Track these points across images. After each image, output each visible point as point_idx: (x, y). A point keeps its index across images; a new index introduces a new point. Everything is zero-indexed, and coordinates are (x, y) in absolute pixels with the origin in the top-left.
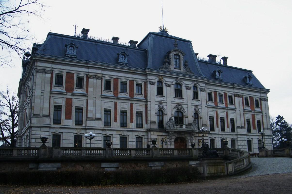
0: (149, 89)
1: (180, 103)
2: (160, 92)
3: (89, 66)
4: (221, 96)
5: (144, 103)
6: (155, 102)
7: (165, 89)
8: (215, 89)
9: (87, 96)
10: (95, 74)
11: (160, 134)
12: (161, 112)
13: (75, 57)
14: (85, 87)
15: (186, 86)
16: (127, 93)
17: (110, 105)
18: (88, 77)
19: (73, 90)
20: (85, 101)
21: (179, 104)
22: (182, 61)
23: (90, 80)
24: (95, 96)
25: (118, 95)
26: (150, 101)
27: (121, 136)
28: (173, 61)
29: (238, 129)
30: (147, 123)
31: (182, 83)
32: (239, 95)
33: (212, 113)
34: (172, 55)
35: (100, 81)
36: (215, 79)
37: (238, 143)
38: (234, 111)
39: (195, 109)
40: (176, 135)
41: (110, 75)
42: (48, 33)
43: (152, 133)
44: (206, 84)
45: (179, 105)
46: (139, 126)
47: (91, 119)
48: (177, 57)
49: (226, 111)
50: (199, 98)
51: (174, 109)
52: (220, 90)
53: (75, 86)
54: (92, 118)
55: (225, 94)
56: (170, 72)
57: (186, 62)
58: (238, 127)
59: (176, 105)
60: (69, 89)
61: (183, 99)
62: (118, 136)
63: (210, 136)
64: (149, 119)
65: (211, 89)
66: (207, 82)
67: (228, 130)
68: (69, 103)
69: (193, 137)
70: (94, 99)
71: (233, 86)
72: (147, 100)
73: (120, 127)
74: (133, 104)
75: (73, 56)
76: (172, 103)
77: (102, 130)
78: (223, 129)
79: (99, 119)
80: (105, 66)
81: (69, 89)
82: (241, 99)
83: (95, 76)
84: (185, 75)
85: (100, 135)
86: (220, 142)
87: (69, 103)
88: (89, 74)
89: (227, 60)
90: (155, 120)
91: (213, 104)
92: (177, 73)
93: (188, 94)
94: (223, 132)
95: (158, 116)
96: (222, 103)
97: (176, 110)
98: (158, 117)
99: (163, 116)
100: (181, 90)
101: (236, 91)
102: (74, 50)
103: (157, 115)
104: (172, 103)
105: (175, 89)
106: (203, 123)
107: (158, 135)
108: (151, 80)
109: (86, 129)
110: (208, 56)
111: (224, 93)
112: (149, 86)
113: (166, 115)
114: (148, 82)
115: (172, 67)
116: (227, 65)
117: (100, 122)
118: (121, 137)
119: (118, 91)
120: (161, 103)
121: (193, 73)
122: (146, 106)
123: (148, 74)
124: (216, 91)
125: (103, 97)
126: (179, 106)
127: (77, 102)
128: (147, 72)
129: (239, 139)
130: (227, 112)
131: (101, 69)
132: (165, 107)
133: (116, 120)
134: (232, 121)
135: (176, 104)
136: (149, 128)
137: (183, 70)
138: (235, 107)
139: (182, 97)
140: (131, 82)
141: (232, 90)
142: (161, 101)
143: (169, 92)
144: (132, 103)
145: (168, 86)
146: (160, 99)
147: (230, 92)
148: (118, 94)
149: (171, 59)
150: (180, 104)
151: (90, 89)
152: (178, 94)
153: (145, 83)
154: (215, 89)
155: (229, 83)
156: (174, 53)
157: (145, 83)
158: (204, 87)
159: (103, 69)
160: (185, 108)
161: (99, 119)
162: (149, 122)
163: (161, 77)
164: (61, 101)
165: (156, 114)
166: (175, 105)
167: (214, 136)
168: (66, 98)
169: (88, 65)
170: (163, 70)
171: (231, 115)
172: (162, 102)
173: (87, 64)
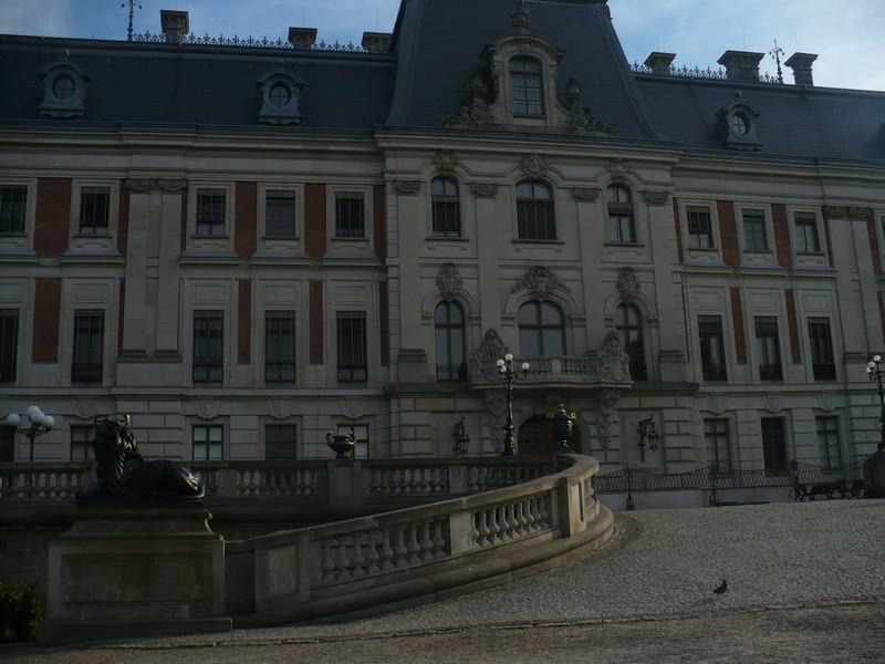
0: (391, 212)
1: (541, 264)
2: (447, 219)
3: (129, 146)
4: (754, 218)
5: (375, 276)
6: (423, 265)
8: (725, 192)
9: (123, 266)
10: (156, 175)
11: (446, 404)
12: (452, 310)
13: (72, 118)
14: (113, 231)
15: (573, 189)
16: (297, 240)
17: (219, 293)
18: (126, 190)
20: (114, 286)
21: (538, 271)
22: (552, 83)
23: (135, 199)
24: (153, 262)
25: (254, 250)
26: (398, 266)
27: (270, 422)
28: (506, 86)
29: (848, 366)
30: (385, 361)
31: (551, 174)
32: (848, 208)
33: (712, 300)
34: (502, 59)
35: (178, 198)
36: (725, 146)
37: (853, 431)
38: (829, 285)
39: (619, 286)
40: (527, 409)
41: (219, 168)
43: (407, 403)
44: (675, 170)
45: (539, 272)
48: (529, 67)
49: (783, 285)
50: (642, 236)
51: (513, 292)
52: (750, 194)
53: (74, 229)
54: (143, 352)
55: (779, 210)
56: (496, 131)
57: (572, 82)
58: (847, 357)
59: (527, 276)
60: (51, 243)
61: (558, 247)
62: (254, 422)
63: (703, 404)
64: (393, 342)
65: (704, 190)
66: (676, 160)
67: (799, 373)
68: (48, 294)
69: (606, 411)
70: (152, 272)
71: (817, 170)
72: (384, 262)
73: (263, 384)
74: (321, 281)
75: (69, 115)
76: (501, 267)
77: (183, 398)
78: (772, 373)
79: (172, 356)
80: (196, 139)
82: (861, 226)
83: (157, 180)
84: (567, 135)
85: (171, 421)
86: (758, 428)
87: (48, 294)
88: (133, 175)
89: (816, 67)
90: (421, 348)
91: (713, 258)
92: (526, 134)
93: (581, 223)
94: (769, 382)
95: (438, 326)
96: (766, 250)
97: (528, 298)
98: (445, 331)
99: (462, 326)
100: (549, 205)
101: (831, 190)
102: (73, 90)
103: (432, 322)
104: (501, 267)
105: (520, 203)
106: (663, 349)
107: (433, 412)
108: (399, 177)
109: (114, 398)
110: (721, 61)
111: (772, 204)
112: (391, 199)
113: (475, 322)
114: (389, 186)
115: (499, 113)
116: (815, 84)
117: (173, 367)
118: (267, 426)
119: (255, 236)
120: (448, 267)
121: (608, 131)
122: (383, 287)
123: (386, 153)
124: (731, 197)
125: (186, 263)
126: (541, 276)
127: (79, 291)
128: (381, 145)
129: (856, 412)
130: (789, 294)
131: (182, 151)
132: (469, 286)
133: (244, 357)
134: (820, 330)
135: (525, 267)
136: (392, 381)
137: (557, 118)
138: (831, 264)
139: (555, 238)
140: (315, 192)
141: (814, 190)
142: (450, 261)
143: (491, 220)
144: (318, 279)
145: (485, 191)
146: (447, 251)
147: (801, 197)
148: (254, 243)
149: (497, 77)
150: (544, 268)
151: (134, 237)
152: (537, 222)
153: (379, 190)
154: (725, 192)
155: (795, 158)
156: (512, 50)
157: (379, 190)
158: (666, 185)
159: (188, 151)
160: (568, 284)
161: (172, 356)
162: (393, 354)
163: (447, 159)
165: (424, 318)
166: (521, 273)
167: (722, 406)
168: (37, 279)
169: (126, 142)
170: (458, 127)
171: (814, 302)
172: (452, 265)
173: (120, 137)
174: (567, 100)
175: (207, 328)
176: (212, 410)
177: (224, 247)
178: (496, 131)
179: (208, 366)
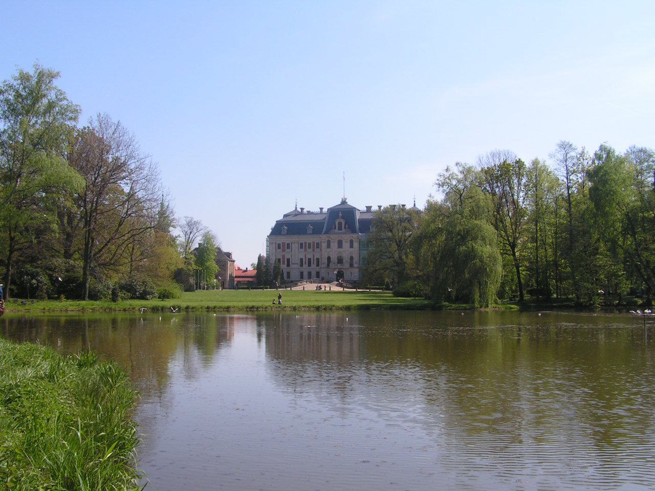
2: (329, 246)
7: (332, 244)
19: (285, 251)
42: (290, 209)
46: (318, 265)
47: (294, 264)
60: (284, 251)
68: (284, 257)
81: (284, 251)
87: (284, 257)
93: (346, 245)
115: (336, 231)
127: (288, 256)
140: (314, 243)
146: (328, 250)
152: (340, 244)
164: (281, 257)
174: (345, 228)
175: (301, 260)
176: (302, 270)
177: (303, 250)
178: (335, 233)
179: (302, 265)
